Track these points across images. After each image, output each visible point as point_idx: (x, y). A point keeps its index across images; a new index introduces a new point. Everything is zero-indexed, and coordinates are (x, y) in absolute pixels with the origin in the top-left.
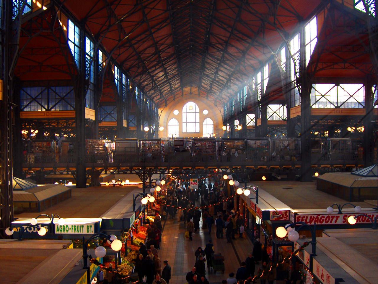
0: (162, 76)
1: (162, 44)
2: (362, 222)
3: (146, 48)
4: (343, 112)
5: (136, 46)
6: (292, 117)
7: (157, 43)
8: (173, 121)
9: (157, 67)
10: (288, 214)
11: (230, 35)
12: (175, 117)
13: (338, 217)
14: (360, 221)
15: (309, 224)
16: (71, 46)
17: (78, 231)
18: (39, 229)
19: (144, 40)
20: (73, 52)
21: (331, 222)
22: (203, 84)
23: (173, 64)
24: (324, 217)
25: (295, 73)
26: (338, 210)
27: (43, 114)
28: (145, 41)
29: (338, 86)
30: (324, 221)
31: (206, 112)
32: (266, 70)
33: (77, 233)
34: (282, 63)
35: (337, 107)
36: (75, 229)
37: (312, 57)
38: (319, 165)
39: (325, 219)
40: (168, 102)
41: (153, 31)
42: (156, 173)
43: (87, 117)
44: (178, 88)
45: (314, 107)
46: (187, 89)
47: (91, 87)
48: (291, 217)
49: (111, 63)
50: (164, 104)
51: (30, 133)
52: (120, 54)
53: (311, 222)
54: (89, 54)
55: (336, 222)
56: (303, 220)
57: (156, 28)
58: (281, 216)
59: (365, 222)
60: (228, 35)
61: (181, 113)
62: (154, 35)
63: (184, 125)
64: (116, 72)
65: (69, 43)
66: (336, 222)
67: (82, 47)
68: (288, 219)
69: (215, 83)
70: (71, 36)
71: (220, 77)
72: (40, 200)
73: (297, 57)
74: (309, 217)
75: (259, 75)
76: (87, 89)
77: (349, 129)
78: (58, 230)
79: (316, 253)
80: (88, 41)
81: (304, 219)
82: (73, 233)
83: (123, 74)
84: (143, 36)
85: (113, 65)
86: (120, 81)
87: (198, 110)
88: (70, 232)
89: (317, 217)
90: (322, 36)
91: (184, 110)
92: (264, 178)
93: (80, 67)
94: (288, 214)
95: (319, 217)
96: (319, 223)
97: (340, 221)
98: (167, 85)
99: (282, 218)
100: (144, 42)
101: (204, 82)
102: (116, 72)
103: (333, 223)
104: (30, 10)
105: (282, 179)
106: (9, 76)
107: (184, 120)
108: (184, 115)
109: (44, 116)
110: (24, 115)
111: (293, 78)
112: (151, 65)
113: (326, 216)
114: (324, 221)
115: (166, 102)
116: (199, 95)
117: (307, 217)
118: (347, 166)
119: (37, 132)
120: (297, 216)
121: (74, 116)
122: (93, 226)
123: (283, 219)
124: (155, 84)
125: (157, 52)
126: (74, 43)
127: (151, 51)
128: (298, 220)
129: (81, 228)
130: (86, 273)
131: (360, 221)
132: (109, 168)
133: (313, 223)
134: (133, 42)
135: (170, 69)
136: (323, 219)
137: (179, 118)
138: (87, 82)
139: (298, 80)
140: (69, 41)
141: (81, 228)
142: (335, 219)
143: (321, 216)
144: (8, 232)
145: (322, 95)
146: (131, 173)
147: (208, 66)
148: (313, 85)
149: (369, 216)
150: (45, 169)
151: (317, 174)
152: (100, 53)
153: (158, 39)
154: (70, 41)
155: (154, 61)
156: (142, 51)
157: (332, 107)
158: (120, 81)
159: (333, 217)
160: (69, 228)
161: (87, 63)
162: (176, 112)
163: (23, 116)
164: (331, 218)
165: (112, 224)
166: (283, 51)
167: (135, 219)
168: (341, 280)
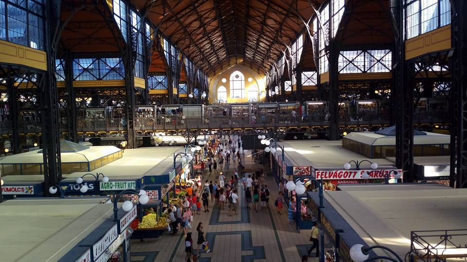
0: (209, 48)
1: (207, 18)
2: (379, 178)
3: (191, 23)
4: (370, 76)
5: (182, 20)
6: (322, 82)
7: (202, 17)
8: (222, 89)
9: (204, 39)
10: (309, 169)
11: (267, 9)
12: (224, 84)
13: (355, 173)
14: (377, 177)
15: (328, 178)
16: (117, 20)
17: (122, 188)
18: (81, 188)
19: (189, 14)
20: (119, 26)
21: (349, 177)
22: (247, 54)
23: (219, 36)
24: (342, 172)
26: (356, 167)
27: (95, 83)
28: (190, 15)
29: (366, 53)
30: (343, 176)
31: (250, 80)
32: (301, 40)
33: (120, 189)
34: (314, 33)
35: (364, 72)
36: (119, 186)
37: (340, 25)
38: (346, 126)
39: (343, 174)
40: (216, 72)
42: (200, 134)
43: (136, 85)
44: (224, 59)
45: (341, 72)
46: (233, 60)
47: (139, 57)
48: (312, 173)
49: (159, 36)
50: (213, 73)
51: (84, 102)
52: (166, 29)
53: (330, 177)
54: (136, 27)
55: (354, 177)
56: (322, 175)
57: (199, 2)
58: (304, 171)
59: (383, 178)
60: (265, 8)
61: (228, 80)
62: (199, 9)
63: (231, 91)
64: (165, 44)
65: (115, 16)
66: (354, 177)
67: (128, 22)
68: (310, 174)
69: (257, 53)
70: (116, 10)
71: (262, 48)
72: (89, 161)
74: (328, 172)
75: (295, 45)
76: (135, 60)
77: (376, 92)
78: (102, 187)
79: (324, 205)
80: (134, 15)
81: (324, 174)
82: (117, 189)
83: (172, 47)
84: (188, 10)
85: (162, 38)
86: (170, 53)
87: (243, 78)
88: (114, 189)
89: (336, 173)
91: (231, 79)
92: (296, 138)
93: (128, 41)
94: (309, 169)
95: (338, 173)
96: (338, 178)
97: (358, 176)
98: (215, 56)
99: (304, 173)
100: (189, 16)
102: (165, 44)
103: (351, 178)
105: (313, 139)
106: (52, 48)
107: (231, 87)
108: (231, 83)
109: (96, 85)
110: (76, 84)
111: (323, 47)
112: (199, 37)
113: (344, 171)
114: (343, 176)
115: (214, 71)
116: (244, 65)
117: (326, 173)
118: (373, 126)
119: (90, 99)
120: (316, 171)
121: (124, 85)
122: (135, 182)
123: (305, 174)
124: (203, 55)
126: (120, 17)
127: (196, 24)
128: (318, 175)
129: (124, 185)
130: (115, 227)
131: (377, 177)
132: (157, 131)
133: (332, 178)
134: (179, 16)
135: (216, 41)
136: (341, 174)
137: (227, 85)
138: (135, 54)
139: (326, 48)
140: (115, 15)
141: (124, 185)
142: (353, 174)
143: (339, 171)
144: (53, 191)
145: (349, 61)
146: (177, 135)
147: (250, 38)
148: (341, 52)
149: (387, 172)
150: (99, 132)
151: (345, 134)
152: (148, 27)
153: (202, 13)
154: (116, 15)
155: (200, 34)
156: (187, 25)
157: (360, 72)
158: (170, 53)
159: (351, 173)
160: (113, 184)
161: (134, 36)
162: (224, 80)
163: (75, 85)
164: (349, 174)
165: (153, 180)
166: (315, 22)
167: (176, 175)
168: (342, 231)
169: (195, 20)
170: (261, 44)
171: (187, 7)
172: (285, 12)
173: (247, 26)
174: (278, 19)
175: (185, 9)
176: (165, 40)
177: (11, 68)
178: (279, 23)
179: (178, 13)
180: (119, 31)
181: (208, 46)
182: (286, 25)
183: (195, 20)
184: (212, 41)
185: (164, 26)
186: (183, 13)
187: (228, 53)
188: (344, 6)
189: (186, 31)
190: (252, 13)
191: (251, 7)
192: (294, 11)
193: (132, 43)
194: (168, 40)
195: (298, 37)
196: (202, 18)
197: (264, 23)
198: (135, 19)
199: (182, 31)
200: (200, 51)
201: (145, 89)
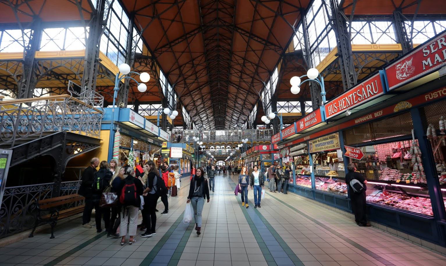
3: (198, 99)
25: (269, 97)
28: (198, 94)
32: (255, 108)
35: (289, 112)
37: (277, 86)
41: (201, 88)
73: (269, 92)
84: (196, 90)
85: (182, 105)
90: (279, 76)
101: (226, 125)
104: (141, 53)
125: (203, 103)
134: (192, 93)
138: (169, 102)
148: (278, 102)
152: (175, 96)
153: (204, 95)
169: (199, 99)
170: (234, 117)
171: (196, 89)
172: (247, 92)
173: (226, 106)
174: (244, 98)
175: (195, 90)
176: (183, 107)
177: (107, 72)
178: (244, 100)
179: (192, 91)
180: (162, 89)
181: (205, 118)
182: (248, 101)
183: (199, 99)
184: (208, 115)
185: (184, 98)
186: (194, 92)
187: (215, 125)
188: (278, 76)
189: (194, 105)
190: (229, 96)
191: (229, 92)
192: (251, 91)
193: (167, 97)
194: (186, 108)
195: (253, 107)
196: (203, 98)
197: (236, 102)
198: (170, 89)
199: (192, 104)
200: (201, 121)
201: (172, 125)
